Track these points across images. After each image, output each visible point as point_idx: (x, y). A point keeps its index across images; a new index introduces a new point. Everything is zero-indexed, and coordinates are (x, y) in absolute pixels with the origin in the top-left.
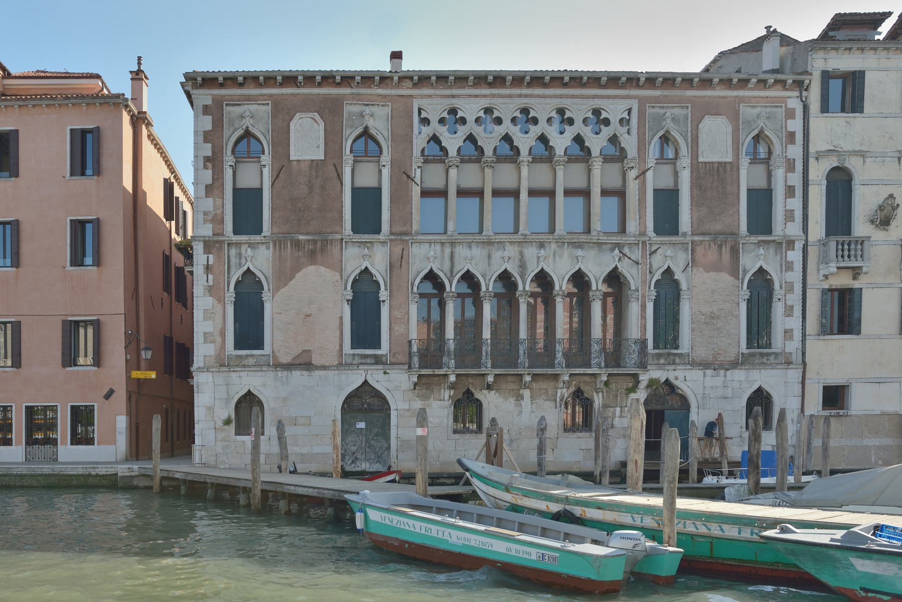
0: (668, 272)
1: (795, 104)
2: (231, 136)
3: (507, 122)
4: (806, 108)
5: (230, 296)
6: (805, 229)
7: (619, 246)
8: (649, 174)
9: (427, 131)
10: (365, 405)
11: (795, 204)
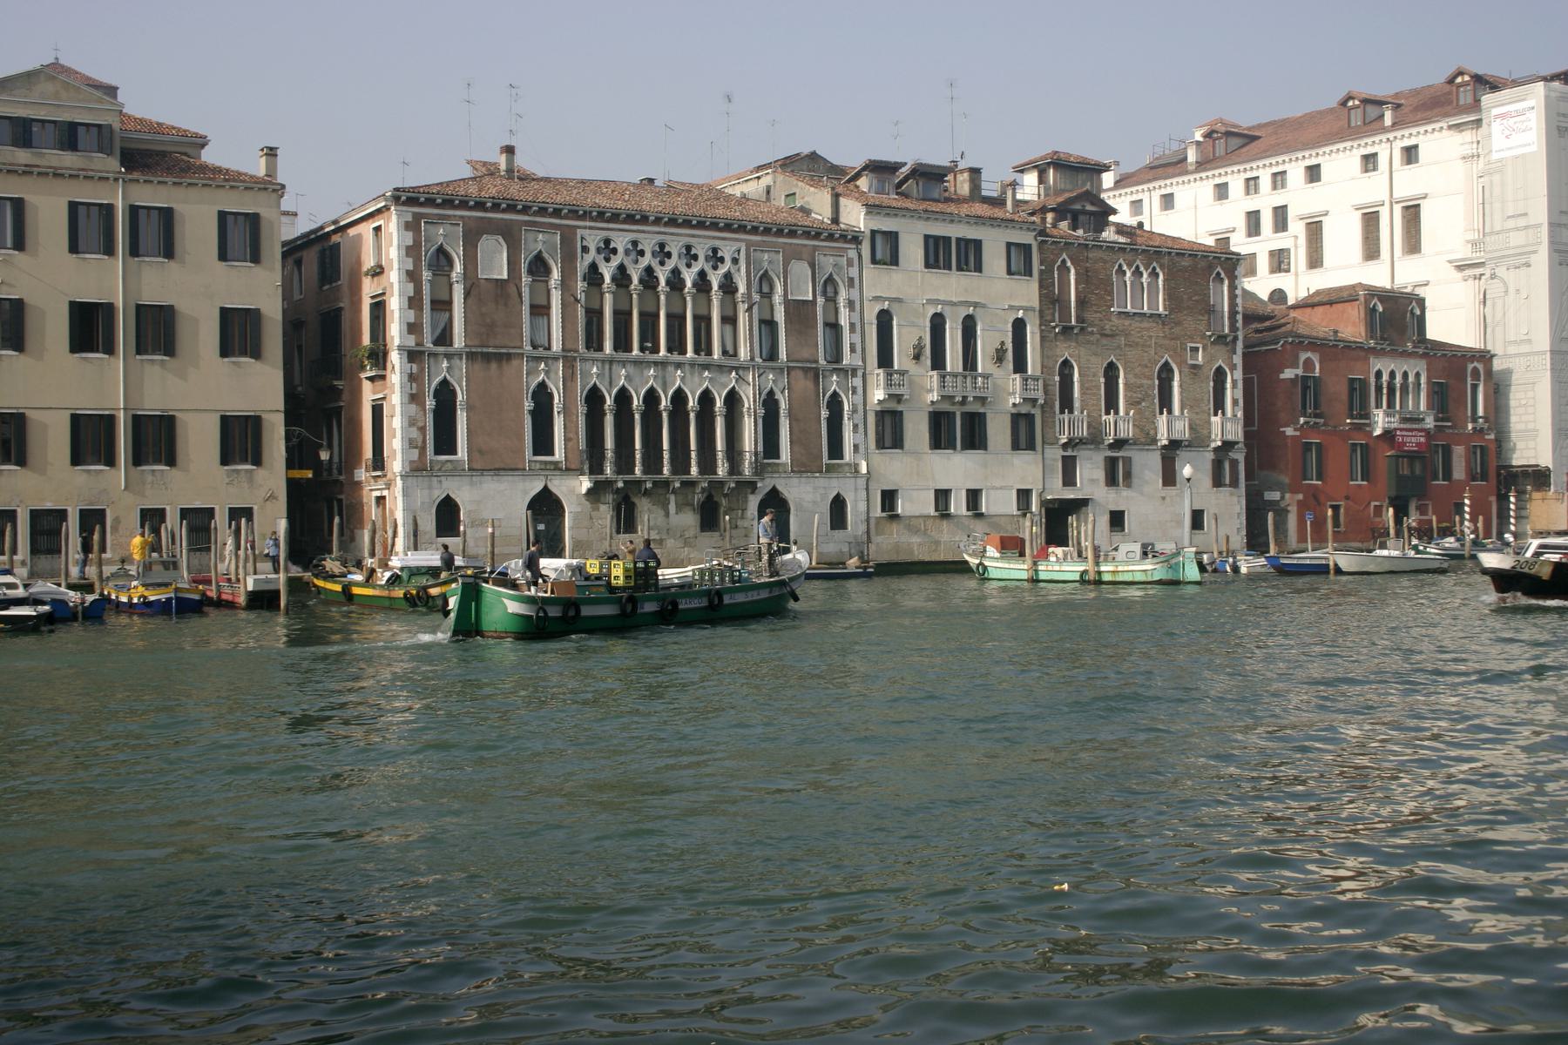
0: (771, 393)
1: (853, 254)
2: (426, 255)
3: (648, 255)
4: (860, 256)
5: (430, 403)
6: (864, 360)
7: (736, 369)
8: (755, 309)
9: (589, 258)
10: (545, 506)
11: (857, 339)
